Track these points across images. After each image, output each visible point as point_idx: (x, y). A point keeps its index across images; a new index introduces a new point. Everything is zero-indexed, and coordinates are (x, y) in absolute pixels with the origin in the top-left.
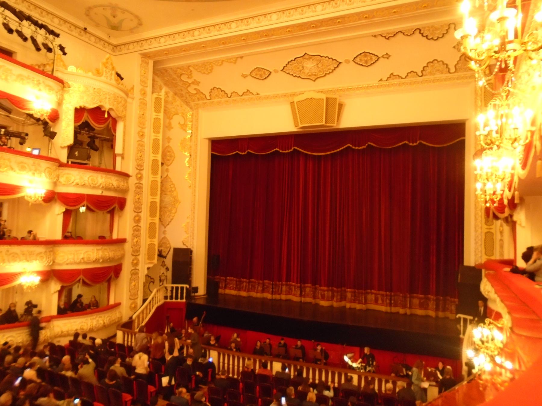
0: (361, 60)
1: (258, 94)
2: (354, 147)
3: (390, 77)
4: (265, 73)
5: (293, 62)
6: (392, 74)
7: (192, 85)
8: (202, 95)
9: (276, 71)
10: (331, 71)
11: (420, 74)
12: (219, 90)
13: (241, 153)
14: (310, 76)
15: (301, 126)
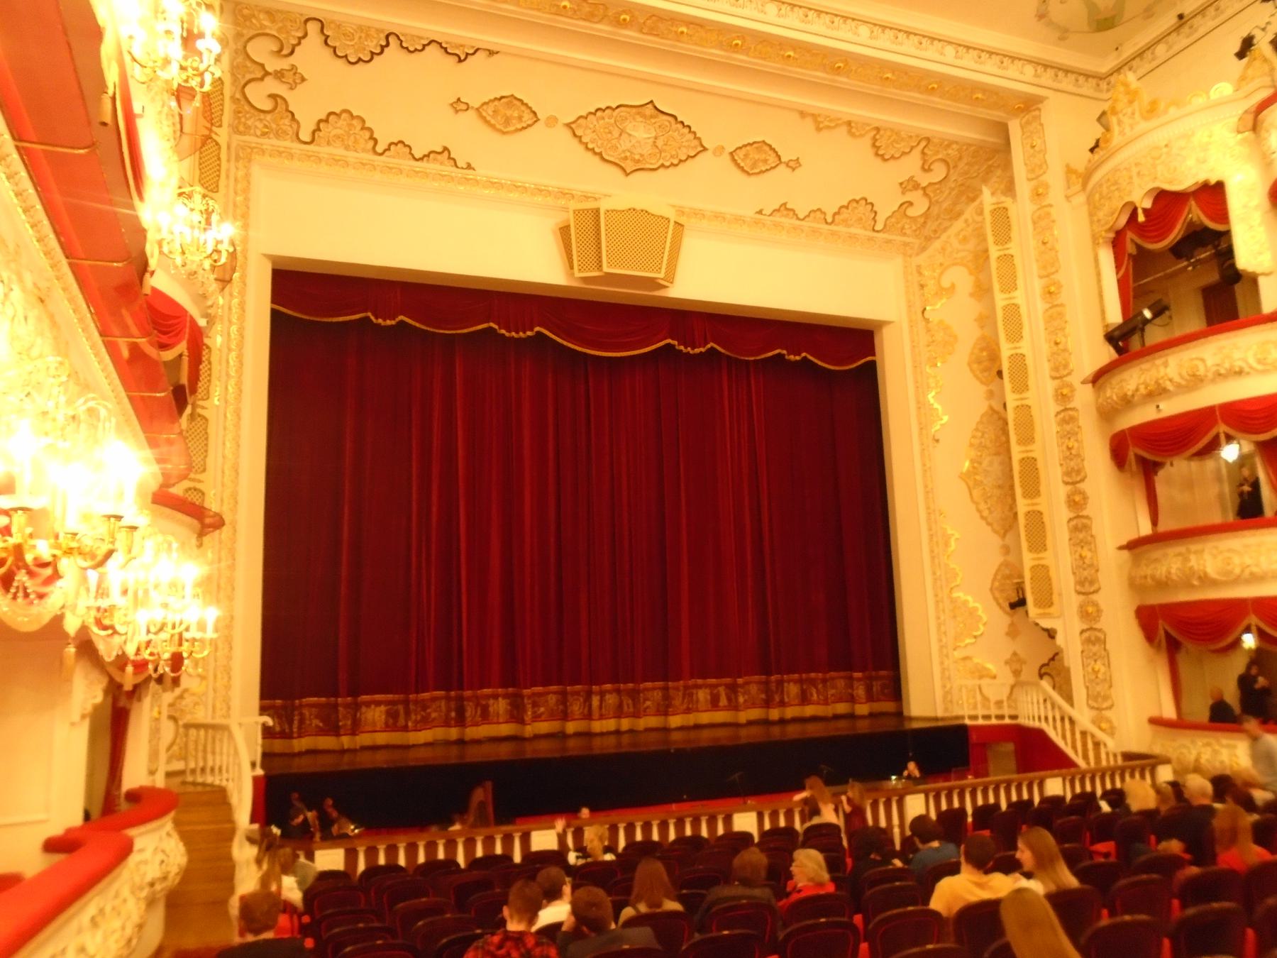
0: (746, 156)
1: (469, 167)
2: (682, 348)
3: (778, 210)
4: (520, 118)
5: (608, 111)
6: (785, 204)
7: (268, 79)
8: (287, 121)
9: (552, 121)
10: (675, 162)
11: (829, 220)
12: (355, 122)
13: (380, 321)
14: (626, 158)
15: (606, 269)
